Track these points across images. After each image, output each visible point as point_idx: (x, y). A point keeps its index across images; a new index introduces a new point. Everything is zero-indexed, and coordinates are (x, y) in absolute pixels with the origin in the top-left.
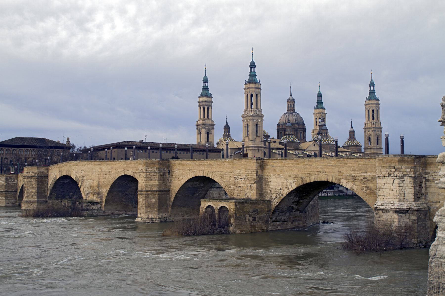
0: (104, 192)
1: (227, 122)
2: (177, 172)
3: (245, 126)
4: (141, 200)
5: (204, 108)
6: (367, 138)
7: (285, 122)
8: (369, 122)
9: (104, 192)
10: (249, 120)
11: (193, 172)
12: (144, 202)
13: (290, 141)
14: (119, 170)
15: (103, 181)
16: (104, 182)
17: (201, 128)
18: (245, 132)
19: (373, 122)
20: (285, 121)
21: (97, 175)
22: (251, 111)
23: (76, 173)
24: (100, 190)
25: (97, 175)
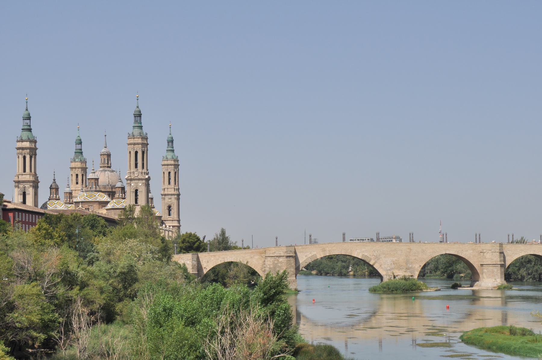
0: (416, 267)
1: (54, 180)
2: (508, 252)
3: (132, 190)
4: (496, 270)
5: (24, 158)
6: (166, 208)
7: (109, 183)
8: (169, 187)
9: (416, 267)
10: (140, 184)
11: (524, 252)
12: (499, 271)
13: (119, 207)
14: (438, 250)
15: (414, 258)
16: (415, 259)
17: (26, 186)
18: (132, 199)
19: (175, 188)
20: (109, 181)
21: (405, 254)
22: (143, 173)
23: (364, 252)
24: (410, 266)
25: (405, 254)
